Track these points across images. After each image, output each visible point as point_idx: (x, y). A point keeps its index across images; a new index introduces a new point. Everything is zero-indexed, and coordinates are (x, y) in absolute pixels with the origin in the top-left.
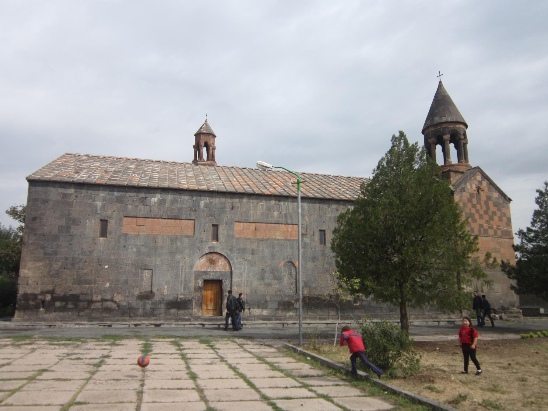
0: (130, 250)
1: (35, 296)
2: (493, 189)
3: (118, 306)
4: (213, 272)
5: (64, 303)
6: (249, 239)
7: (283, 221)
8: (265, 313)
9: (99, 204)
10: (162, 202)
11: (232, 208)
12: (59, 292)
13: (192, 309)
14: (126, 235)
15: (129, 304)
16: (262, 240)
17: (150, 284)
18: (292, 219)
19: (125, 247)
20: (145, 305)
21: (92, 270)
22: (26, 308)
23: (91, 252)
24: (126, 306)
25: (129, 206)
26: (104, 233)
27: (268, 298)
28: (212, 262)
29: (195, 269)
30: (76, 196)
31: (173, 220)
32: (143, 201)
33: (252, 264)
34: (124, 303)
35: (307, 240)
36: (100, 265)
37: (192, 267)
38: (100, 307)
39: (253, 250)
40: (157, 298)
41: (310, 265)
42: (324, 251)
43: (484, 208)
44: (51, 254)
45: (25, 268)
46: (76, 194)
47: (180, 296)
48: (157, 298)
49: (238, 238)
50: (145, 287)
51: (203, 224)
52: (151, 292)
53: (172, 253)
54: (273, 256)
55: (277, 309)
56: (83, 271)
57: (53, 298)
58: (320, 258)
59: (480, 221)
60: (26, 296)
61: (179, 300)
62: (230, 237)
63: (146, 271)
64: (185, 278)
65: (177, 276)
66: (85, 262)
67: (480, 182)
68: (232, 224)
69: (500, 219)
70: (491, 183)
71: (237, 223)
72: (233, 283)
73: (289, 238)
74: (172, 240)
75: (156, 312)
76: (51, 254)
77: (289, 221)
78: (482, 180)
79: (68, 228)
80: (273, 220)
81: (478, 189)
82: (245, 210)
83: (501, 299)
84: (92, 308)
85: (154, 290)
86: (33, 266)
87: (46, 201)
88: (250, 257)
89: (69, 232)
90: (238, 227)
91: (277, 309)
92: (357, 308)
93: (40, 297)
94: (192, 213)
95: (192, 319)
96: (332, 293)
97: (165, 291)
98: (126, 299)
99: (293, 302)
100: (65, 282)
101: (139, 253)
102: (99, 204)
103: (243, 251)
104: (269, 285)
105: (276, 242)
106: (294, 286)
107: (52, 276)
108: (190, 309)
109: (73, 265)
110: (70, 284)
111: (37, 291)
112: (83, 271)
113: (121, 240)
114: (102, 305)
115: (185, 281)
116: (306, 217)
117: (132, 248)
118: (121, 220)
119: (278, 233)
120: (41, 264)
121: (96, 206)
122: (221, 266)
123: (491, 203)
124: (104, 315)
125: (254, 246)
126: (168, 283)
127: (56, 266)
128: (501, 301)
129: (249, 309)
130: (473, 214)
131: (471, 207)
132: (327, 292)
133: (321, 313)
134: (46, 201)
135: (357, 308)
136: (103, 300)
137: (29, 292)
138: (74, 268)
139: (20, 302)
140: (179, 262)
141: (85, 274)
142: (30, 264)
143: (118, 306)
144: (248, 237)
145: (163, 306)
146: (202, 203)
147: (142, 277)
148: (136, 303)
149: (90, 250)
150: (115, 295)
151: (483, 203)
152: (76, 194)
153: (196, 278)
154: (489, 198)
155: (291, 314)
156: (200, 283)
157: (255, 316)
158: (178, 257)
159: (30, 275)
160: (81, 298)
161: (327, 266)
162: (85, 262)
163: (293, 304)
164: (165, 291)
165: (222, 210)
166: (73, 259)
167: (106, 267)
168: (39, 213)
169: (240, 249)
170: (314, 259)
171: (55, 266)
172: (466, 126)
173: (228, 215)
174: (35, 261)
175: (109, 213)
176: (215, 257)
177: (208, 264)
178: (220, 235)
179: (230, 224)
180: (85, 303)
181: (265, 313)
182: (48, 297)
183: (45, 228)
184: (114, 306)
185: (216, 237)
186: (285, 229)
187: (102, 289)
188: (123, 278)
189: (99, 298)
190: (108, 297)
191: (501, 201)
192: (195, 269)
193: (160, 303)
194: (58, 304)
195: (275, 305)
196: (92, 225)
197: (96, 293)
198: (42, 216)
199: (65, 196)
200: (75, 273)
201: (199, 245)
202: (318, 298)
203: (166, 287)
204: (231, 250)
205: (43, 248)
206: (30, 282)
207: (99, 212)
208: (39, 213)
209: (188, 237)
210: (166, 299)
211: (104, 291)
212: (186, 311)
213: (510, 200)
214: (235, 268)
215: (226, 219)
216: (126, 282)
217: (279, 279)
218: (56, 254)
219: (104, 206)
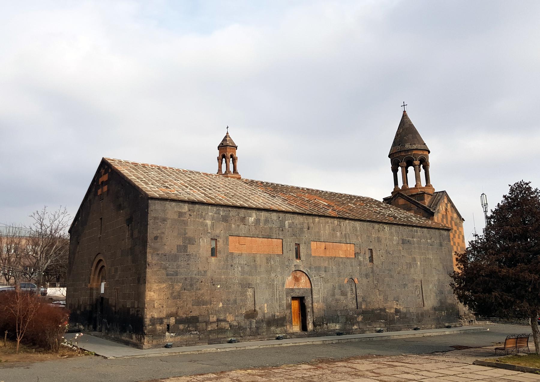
0: (236, 269)
1: (161, 321)
2: (454, 211)
4: (299, 289)
5: (187, 326)
6: (322, 257)
8: (338, 327)
9: (209, 222)
10: (258, 221)
12: (182, 315)
13: (286, 325)
14: (232, 254)
15: (239, 323)
16: (331, 258)
17: (253, 303)
19: (232, 266)
20: (251, 324)
21: (207, 290)
22: (154, 334)
23: (205, 272)
24: (237, 326)
25: (233, 226)
26: (214, 252)
27: (339, 313)
28: (297, 279)
29: (285, 287)
30: (190, 215)
31: (266, 239)
32: (243, 220)
33: (326, 281)
34: (235, 323)
35: (361, 258)
36: (214, 285)
37: (283, 284)
38: (216, 328)
40: (260, 316)
41: (365, 281)
42: (372, 268)
44: (172, 275)
45: (150, 291)
46: (189, 213)
48: (260, 316)
49: (314, 257)
50: (250, 306)
51: (289, 243)
52: (255, 310)
53: (269, 272)
54: (339, 273)
56: (201, 292)
57: (176, 320)
58: (371, 275)
60: (154, 321)
61: (276, 318)
62: (309, 255)
63: (249, 290)
64: (279, 295)
65: (273, 294)
66: (202, 282)
67: (446, 204)
68: (309, 243)
69: (459, 238)
70: (453, 206)
71: (312, 243)
72: (314, 300)
74: (267, 259)
75: (259, 330)
76: (172, 275)
77: (348, 241)
79: (185, 247)
80: (338, 240)
81: (446, 210)
82: (317, 230)
84: (209, 329)
85: (257, 309)
86: (157, 288)
87: (164, 220)
89: (187, 251)
90: (314, 245)
93: (165, 321)
94: (280, 233)
95: (288, 336)
96: (381, 307)
97: (266, 309)
98: (236, 318)
99: (356, 315)
100: (186, 303)
101: (243, 272)
102: (209, 222)
103: (318, 269)
105: (341, 260)
106: (355, 301)
107: (174, 298)
108: (284, 326)
109: (191, 285)
110: (191, 306)
111: (163, 315)
112: (201, 292)
113: (229, 259)
114: (217, 326)
115: (280, 298)
117: (238, 267)
118: (227, 239)
120: (164, 285)
121: (206, 225)
122: (304, 284)
124: (219, 336)
125: (326, 264)
126: (267, 301)
127: (178, 287)
129: (327, 324)
132: (377, 306)
134: (164, 220)
136: (218, 320)
137: (156, 316)
138: (193, 289)
139: (149, 327)
140: (273, 280)
141: (202, 295)
142: (155, 286)
143: (230, 326)
144: (321, 255)
145: (265, 325)
147: (246, 295)
148: (244, 323)
149: (205, 269)
150: (227, 315)
152: (189, 213)
153: (287, 296)
154: (452, 218)
156: (290, 299)
157: (332, 331)
158: (273, 275)
159: (155, 297)
160: (200, 319)
161: (376, 282)
162: (202, 282)
163: (356, 318)
164: (266, 309)
165: (301, 229)
166: (191, 278)
167: (219, 286)
168: (159, 231)
169: (316, 267)
170: (367, 276)
171: (176, 287)
172: (429, 152)
173: (306, 236)
174: (159, 282)
175: (218, 232)
176: (299, 274)
177: (294, 282)
178: (302, 254)
179: (308, 244)
180: (204, 324)
181: (338, 327)
182: (172, 320)
183: (166, 247)
184: (227, 326)
185: (298, 256)
186: (346, 249)
187: (217, 309)
188: (232, 298)
189: (215, 319)
190: (222, 318)
191: (458, 221)
192: (285, 287)
193: (263, 321)
194: (181, 327)
195: (343, 320)
196: (204, 245)
197: (212, 314)
198: (162, 235)
199: (181, 214)
200: (194, 293)
201: (287, 264)
203: (266, 305)
204: (310, 268)
205: (166, 268)
206: (156, 305)
207: (209, 231)
208: (159, 231)
209: (278, 255)
210: (266, 316)
211: (218, 311)
212: (282, 328)
213: (463, 220)
214: (314, 285)
216: (235, 301)
217: (344, 294)
218: (177, 275)
219: (213, 225)
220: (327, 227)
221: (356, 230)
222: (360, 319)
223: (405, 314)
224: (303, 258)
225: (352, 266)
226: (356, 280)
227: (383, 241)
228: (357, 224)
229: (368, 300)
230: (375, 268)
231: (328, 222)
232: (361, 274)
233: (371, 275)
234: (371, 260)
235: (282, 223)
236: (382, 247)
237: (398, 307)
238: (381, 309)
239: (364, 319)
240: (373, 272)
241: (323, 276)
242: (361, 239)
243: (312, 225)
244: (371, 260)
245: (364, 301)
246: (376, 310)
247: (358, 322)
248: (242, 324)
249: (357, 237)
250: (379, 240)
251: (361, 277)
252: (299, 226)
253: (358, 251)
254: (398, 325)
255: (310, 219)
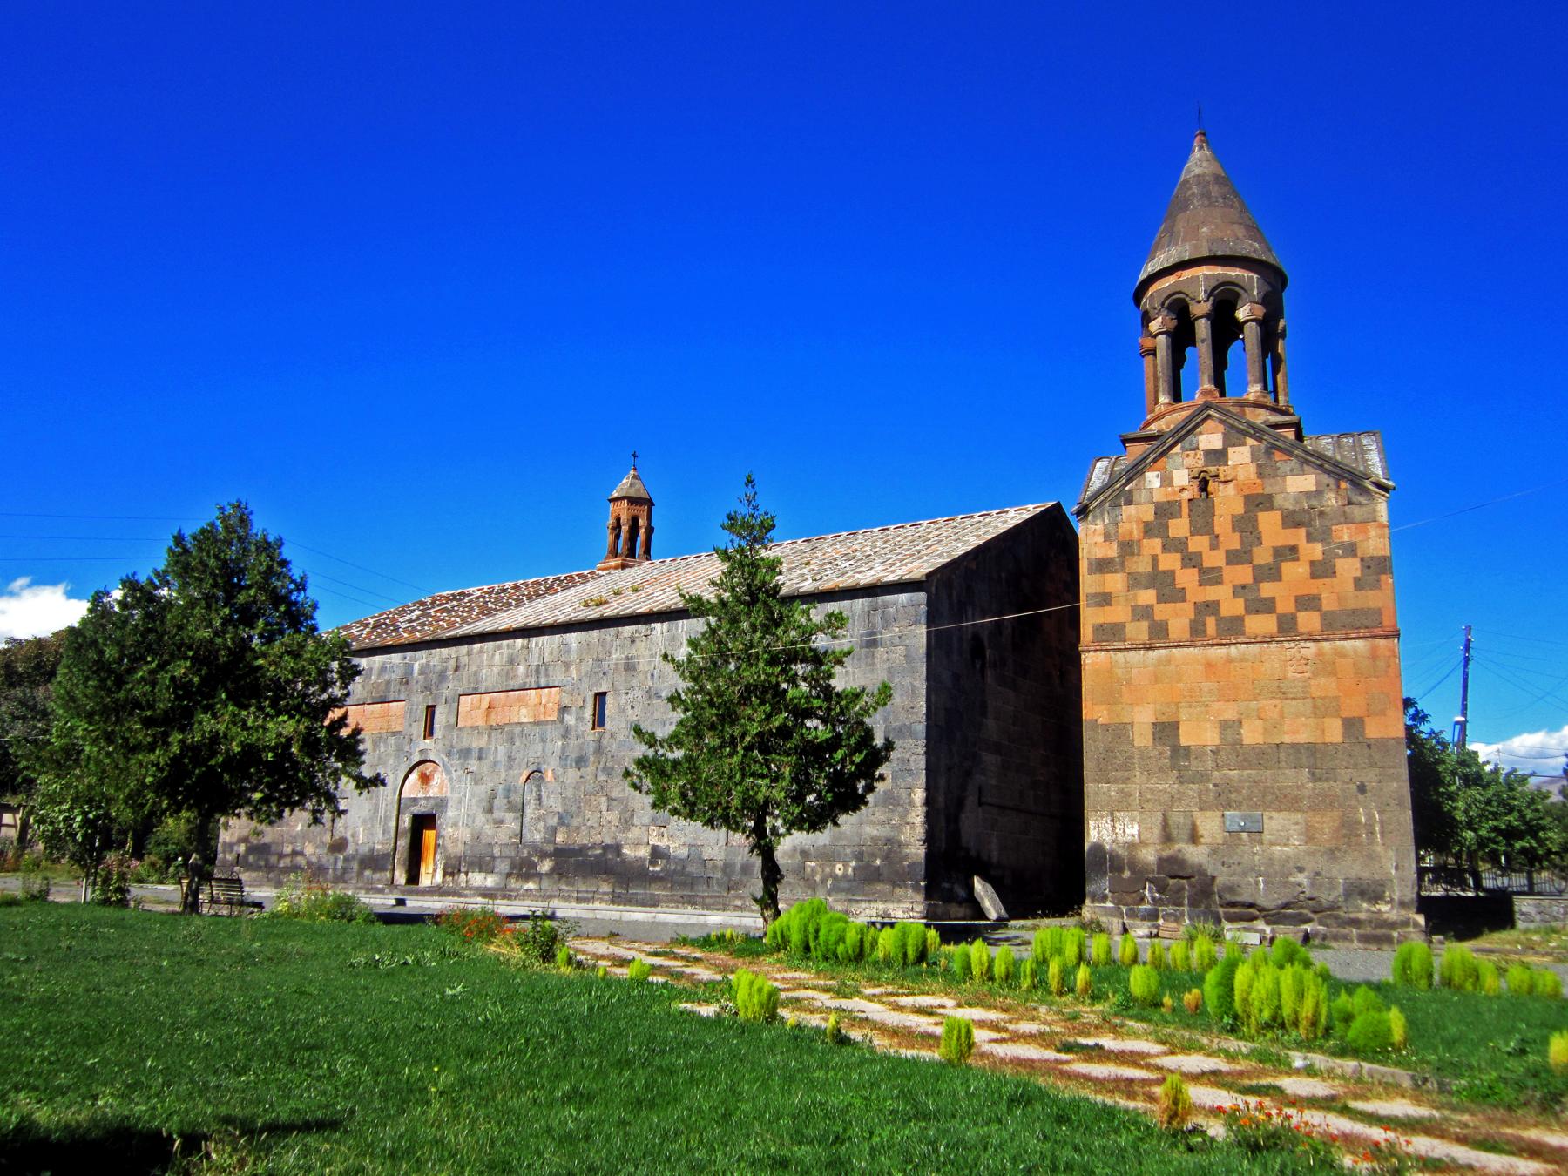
3: (309, 863)
7: (532, 682)
11: (457, 669)
18: (547, 675)
27: (496, 852)
33: (477, 780)
34: (314, 859)
35: (570, 719)
39: (481, 750)
40: (350, 850)
41: (572, 775)
43: (1234, 542)
47: (378, 847)
54: (510, 759)
55: (509, 875)
59: (1198, 595)
65: (376, 810)
73: (542, 718)
78: (1228, 442)
83: (1301, 870)
88: (474, 765)
91: (509, 875)
92: (655, 878)
96: (608, 841)
104: (501, 822)
105: (517, 730)
116: (573, 668)
119: (524, 711)
123: (1268, 522)
125: (483, 743)
128: (1301, 878)
130: (1171, 574)
131: (1158, 550)
132: (598, 839)
133: (583, 888)
135: (655, 878)
136: (295, 853)
145: (355, 865)
146: (416, 667)
148: (327, 859)
151: (1222, 524)
155: (531, 886)
160: (273, 848)
161: (602, 777)
163: (535, 865)
165: (442, 676)
170: (580, 762)
173: (450, 687)
181: (491, 881)
182: (242, 848)
185: (429, 732)
193: (353, 857)
194: (251, 858)
202: (583, 850)
204: (449, 754)
215: (446, 692)
220: (497, 657)
221: (568, 652)
222: (546, 866)
223: (683, 862)
224: (438, 732)
225: (543, 740)
226: (549, 776)
227: (643, 666)
228: (573, 638)
229: (575, 822)
230: (605, 742)
231: (499, 647)
232: (563, 758)
233: (592, 759)
234: (599, 719)
235: (409, 667)
236: (635, 683)
237: (663, 843)
238: (606, 848)
239: (559, 872)
240: (599, 750)
241: (473, 769)
242: (578, 670)
243: (464, 660)
244: (599, 719)
245: (562, 822)
246: (593, 846)
247: (540, 875)
248: (324, 860)
249: (567, 665)
250: (629, 666)
251: (564, 767)
252: (439, 668)
253: (567, 702)
254: (657, 891)
255: (464, 649)
